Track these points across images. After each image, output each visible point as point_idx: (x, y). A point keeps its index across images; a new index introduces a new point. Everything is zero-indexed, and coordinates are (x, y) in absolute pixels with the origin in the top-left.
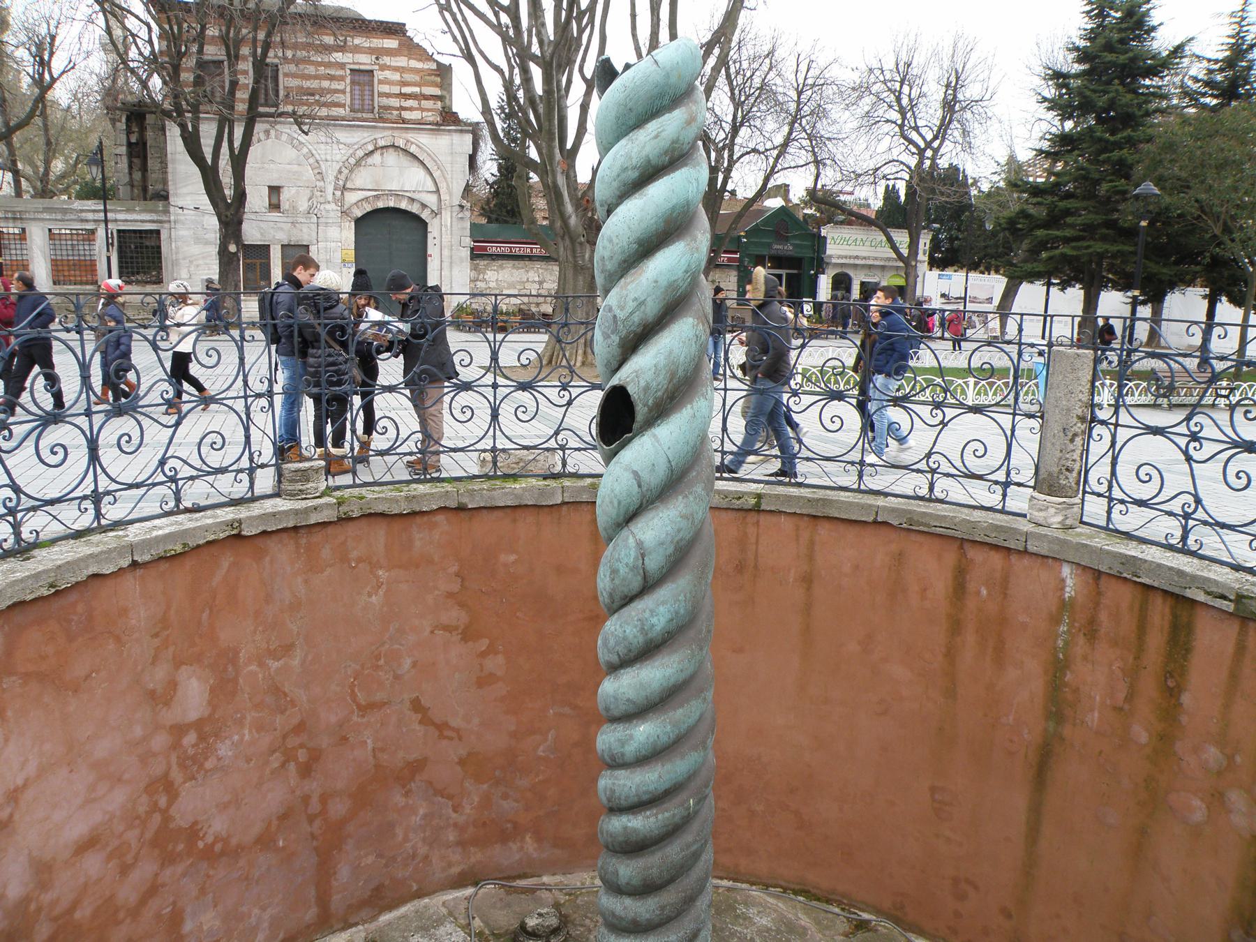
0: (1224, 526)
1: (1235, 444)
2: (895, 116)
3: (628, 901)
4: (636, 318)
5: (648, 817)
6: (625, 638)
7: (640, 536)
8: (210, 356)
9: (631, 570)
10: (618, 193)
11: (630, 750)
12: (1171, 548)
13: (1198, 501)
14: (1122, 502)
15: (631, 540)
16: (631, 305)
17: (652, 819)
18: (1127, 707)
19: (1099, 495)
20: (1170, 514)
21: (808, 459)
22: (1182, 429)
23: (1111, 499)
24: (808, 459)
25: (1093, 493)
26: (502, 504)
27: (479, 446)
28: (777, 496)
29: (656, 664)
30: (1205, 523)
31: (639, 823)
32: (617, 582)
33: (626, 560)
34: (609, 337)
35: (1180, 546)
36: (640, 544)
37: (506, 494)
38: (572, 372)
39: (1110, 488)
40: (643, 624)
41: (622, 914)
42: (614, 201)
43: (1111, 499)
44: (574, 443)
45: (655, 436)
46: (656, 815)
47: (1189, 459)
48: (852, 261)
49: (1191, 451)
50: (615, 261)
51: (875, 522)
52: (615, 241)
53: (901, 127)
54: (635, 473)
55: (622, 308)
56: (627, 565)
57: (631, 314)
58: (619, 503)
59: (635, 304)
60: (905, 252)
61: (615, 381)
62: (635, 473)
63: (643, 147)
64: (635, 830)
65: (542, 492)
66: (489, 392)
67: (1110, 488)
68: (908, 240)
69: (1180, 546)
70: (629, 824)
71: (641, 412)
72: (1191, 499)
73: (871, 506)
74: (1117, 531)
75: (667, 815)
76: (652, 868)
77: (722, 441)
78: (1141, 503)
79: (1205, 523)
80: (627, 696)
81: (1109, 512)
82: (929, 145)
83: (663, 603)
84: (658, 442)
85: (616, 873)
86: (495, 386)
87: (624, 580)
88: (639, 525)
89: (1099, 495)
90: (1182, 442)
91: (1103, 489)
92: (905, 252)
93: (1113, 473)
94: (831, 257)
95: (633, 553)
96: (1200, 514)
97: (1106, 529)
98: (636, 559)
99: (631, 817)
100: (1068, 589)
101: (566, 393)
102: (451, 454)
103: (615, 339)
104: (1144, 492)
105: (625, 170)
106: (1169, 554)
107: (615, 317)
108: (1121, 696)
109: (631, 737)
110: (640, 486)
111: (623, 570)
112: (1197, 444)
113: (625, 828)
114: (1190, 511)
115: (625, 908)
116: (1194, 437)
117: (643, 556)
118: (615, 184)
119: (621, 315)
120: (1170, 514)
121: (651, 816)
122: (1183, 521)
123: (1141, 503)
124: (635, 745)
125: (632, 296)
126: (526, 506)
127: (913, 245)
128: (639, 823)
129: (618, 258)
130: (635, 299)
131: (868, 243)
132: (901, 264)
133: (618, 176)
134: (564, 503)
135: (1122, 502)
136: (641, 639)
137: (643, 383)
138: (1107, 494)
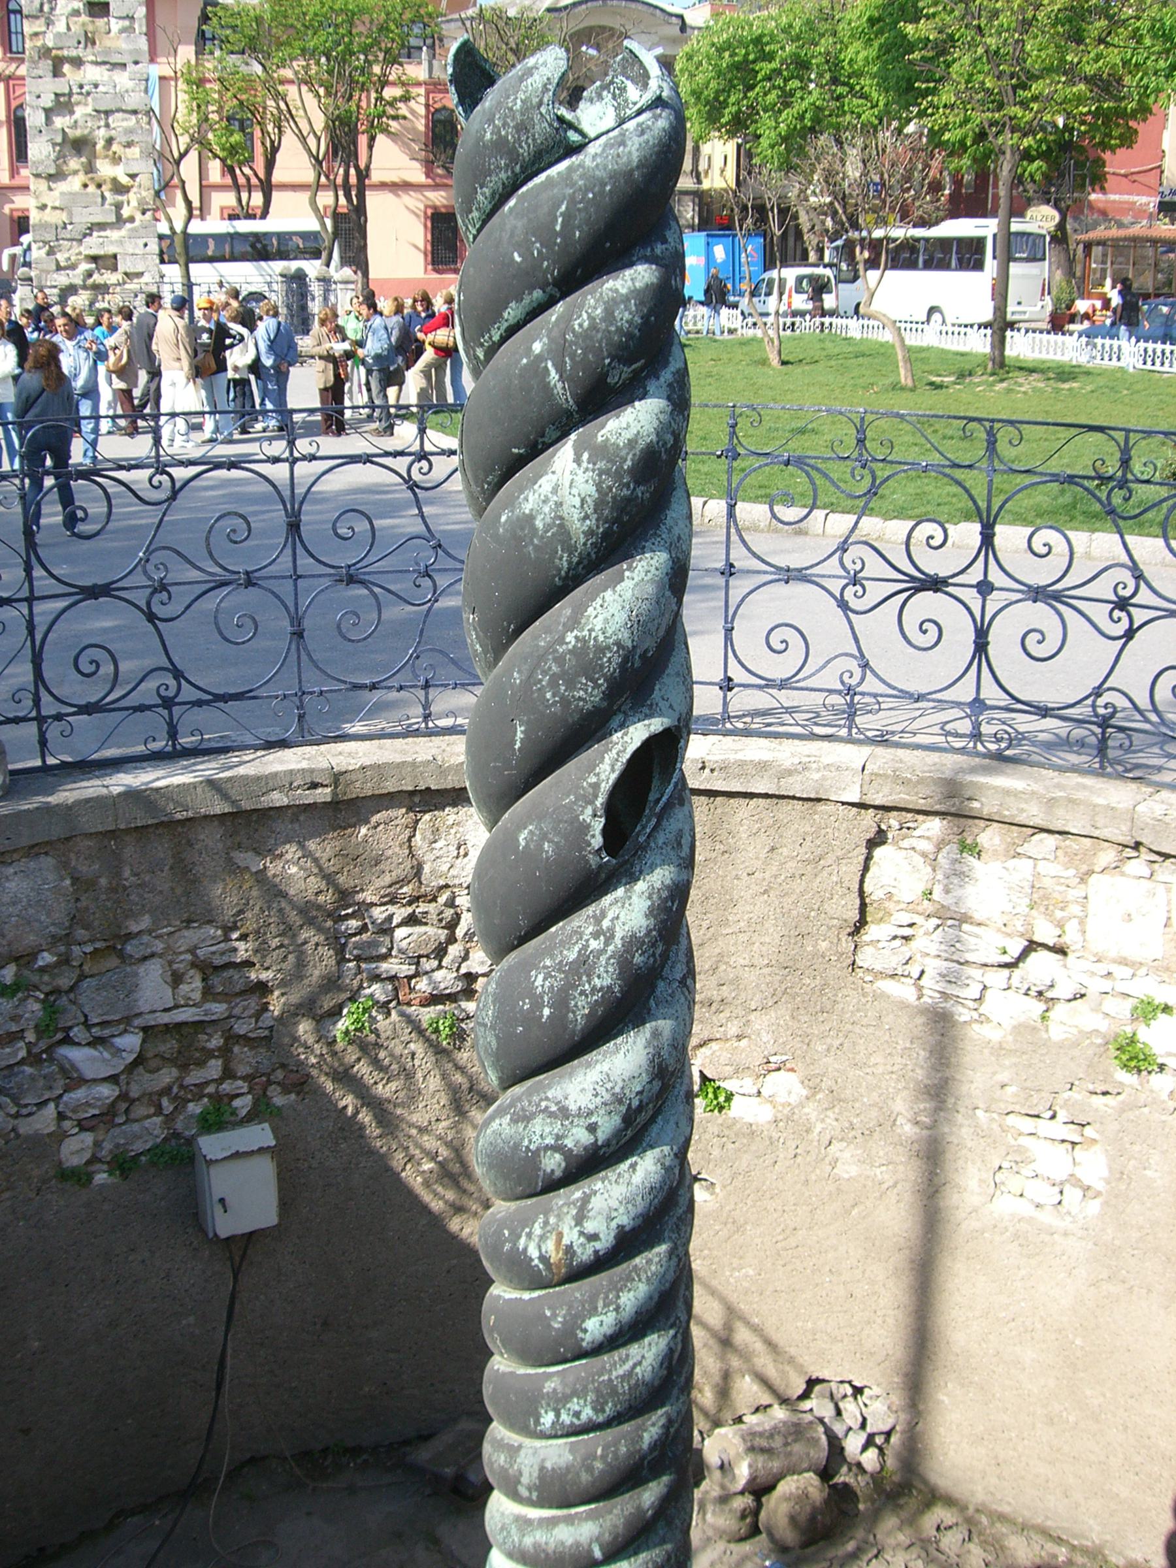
0: (225, 698)
14: (59, 717)
20: (141, 708)
23: (41, 720)
30: (199, 703)
35: (169, 749)
43: (41, 720)
47: (151, 617)
49: (157, 609)
69: (169, 749)
78: (87, 709)
79: (199, 703)
96: (188, 693)
114: (171, 693)
120: (141, 708)
122: (165, 713)
123: (87, 709)
135: (59, 717)
138: (34, 714)
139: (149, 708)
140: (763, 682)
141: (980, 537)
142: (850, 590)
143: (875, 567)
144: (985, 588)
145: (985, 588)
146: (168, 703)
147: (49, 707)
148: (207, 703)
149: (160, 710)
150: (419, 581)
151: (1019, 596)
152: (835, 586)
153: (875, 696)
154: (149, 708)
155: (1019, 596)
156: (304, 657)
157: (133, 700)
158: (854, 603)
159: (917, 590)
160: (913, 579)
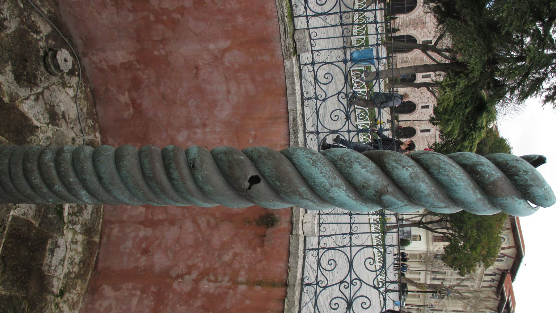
8: (335, 116)
12: (303, 279)
13: (325, 288)
14: (318, 254)
19: (319, 243)
20: (317, 277)
23: (318, 249)
30: (316, 292)
43: (318, 249)
69: (304, 283)
72: (324, 285)
79: (316, 292)
81: (312, 249)
89: (319, 243)
91: (322, 245)
93: (329, 249)
104: (324, 263)
120: (317, 277)
135: (318, 254)
138: (320, 247)
146: (317, 284)
149: (316, 281)
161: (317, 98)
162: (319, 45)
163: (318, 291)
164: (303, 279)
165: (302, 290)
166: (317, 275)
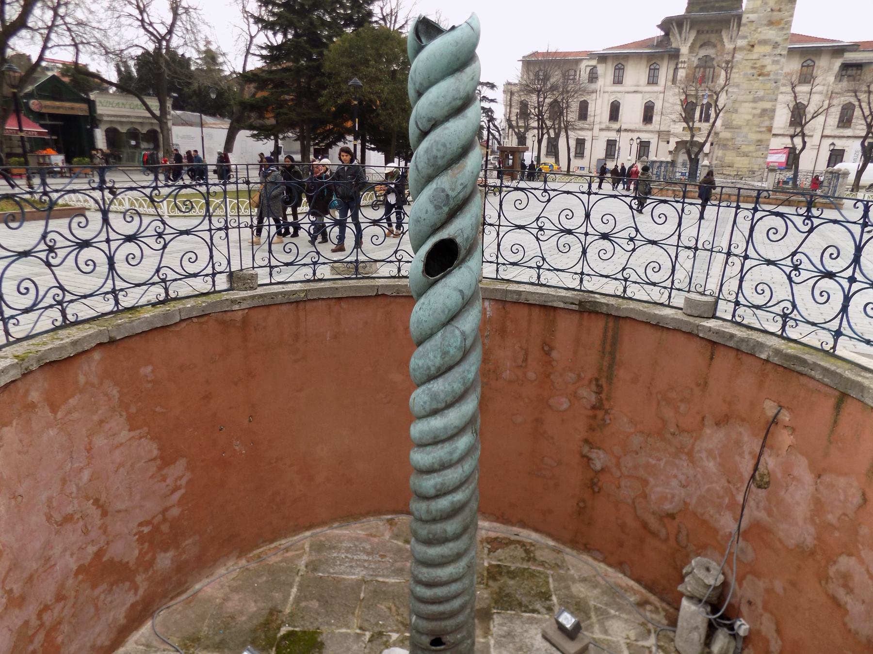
0: (558, 270)
1: (562, 231)
2: (136, 12)
3: (451, 545)
4: (461, 196)
5: (464, 491)
6: (453, 391)
7: (463, 328)
9: (458, 350)
10: (446, 114)
11: (456, 456)
12: (532, 284)
14: (504, 264)
15: (457, 332)
16: (460, 188)
17: (467, 491)
18: (524, 364)
19: (491, 262)
20: (530, 267)
21: (324, 263)
22: (534, 225)
23: (498, 264)
24: (324, 263)
25: (488, 262)
26: (140, 331)
27: (104, 290)
28: (317, 290)
29: (469, 400)
30: (549, 270)
31: (458, 497)
32: (447, 359)
33: (455, 345)
34: (441, 208)
36: (463, 333)
37: (142, 322)
38: (164, 223)
39: (497, 257)
40: (464, 380)
41: (450, 553)
42: (442, 119)
43: (498, 264)
44: (171, 275)
45: (469, 267)
46: (468, 488)
47: (538, 239)
48: (119, 119)
49: (539, 236)
50: (445, 160)
51: (377, 296)
52: (448, 146)
53: (142, 21)
54: (461, 291)
55: (453, 190)
56: (455, 347)
57: (459, 193)
58: (449, 310)
59: (462, 187)
60: (157, 113)
61: (444, 234)
62: (461, 291)
63: (467, 85)
64: (459, 501)
65: (166, 315)
66: (104, 246)
67: (497, 257)
68: (158, 104)
69: (537, 282)
70: (455, 499)
71: (462, 252)
73: (374, 286)
74: (503, 279)
75: (473, 485)
76: (467, 518)
77: (269, 260)
79: (549, 270)
80: (454, 425)
81: (497, 271)
82: (163, 38)
83: (473, 364)
84: (472, 270)
85: (445, 531)
86: (108, 241)
87: (453, 356)
88: (461, 322)
89: (491, 262)
90: (535, 231)
91: (494, 259)
92: (157, 113)
94: (101, 115)
95: (459, 340)
96: (546, 266)
97: (497, 279)
98: (461, 342)
99: (454, 495)
100: (488, 313)
101: (162, 240)
102: (83, 300)
103: (446, 209)
105: (455, 99)
106: (535, 287)
107: (448, 195)
108: (520, 361)
109: (457, 448)
110: (463, 299)
111: (452, 351)
112: (542, 232)
113: (452, 503)
115: (451, 549)
116: (541, 229)
117: (465, 339)
118: (447, 108)
119: (452, 194)
120: (530, 267)
121: (466, 489)
124: (460, 452)
125: (460, 182)
126: (157, 328)
127: (163, 108)
128: (458, 497)
129: (448, 157)
130: (462, 184)
131: (127, 106)
132: (155, 121)
133: (450, 103)
134: (182, 321)
135: (504, 264)
136: (462, 390)
137: (465, 236)
139: (533, 268)
140: (750, 305)
141: (853, 256)
142: (794, 273)
143: (806, 264)
144: (852, 280)
145: (852, 280)
146: (539, 268)
147: (501, 260)
148: (551, 270)
150: (629, 243)
151: (868, 286)
152: (788, 270)
153: (795, 320)
154: (533, 268)
155: (868, 286)
156: (585, 262)
157: (528, 264)
158: (795, 279)
159: (823, 277)
160: (821, 272)
161: (315, 263)
162: (247, 263)
163: (548, 267)
164: (532, 284)
165: (544, 285)
166: (528, 267)
